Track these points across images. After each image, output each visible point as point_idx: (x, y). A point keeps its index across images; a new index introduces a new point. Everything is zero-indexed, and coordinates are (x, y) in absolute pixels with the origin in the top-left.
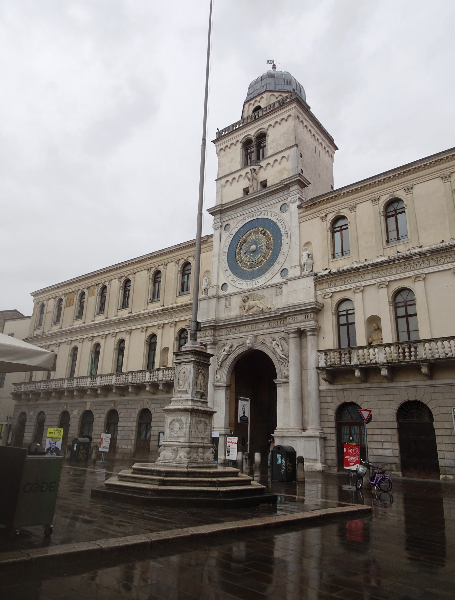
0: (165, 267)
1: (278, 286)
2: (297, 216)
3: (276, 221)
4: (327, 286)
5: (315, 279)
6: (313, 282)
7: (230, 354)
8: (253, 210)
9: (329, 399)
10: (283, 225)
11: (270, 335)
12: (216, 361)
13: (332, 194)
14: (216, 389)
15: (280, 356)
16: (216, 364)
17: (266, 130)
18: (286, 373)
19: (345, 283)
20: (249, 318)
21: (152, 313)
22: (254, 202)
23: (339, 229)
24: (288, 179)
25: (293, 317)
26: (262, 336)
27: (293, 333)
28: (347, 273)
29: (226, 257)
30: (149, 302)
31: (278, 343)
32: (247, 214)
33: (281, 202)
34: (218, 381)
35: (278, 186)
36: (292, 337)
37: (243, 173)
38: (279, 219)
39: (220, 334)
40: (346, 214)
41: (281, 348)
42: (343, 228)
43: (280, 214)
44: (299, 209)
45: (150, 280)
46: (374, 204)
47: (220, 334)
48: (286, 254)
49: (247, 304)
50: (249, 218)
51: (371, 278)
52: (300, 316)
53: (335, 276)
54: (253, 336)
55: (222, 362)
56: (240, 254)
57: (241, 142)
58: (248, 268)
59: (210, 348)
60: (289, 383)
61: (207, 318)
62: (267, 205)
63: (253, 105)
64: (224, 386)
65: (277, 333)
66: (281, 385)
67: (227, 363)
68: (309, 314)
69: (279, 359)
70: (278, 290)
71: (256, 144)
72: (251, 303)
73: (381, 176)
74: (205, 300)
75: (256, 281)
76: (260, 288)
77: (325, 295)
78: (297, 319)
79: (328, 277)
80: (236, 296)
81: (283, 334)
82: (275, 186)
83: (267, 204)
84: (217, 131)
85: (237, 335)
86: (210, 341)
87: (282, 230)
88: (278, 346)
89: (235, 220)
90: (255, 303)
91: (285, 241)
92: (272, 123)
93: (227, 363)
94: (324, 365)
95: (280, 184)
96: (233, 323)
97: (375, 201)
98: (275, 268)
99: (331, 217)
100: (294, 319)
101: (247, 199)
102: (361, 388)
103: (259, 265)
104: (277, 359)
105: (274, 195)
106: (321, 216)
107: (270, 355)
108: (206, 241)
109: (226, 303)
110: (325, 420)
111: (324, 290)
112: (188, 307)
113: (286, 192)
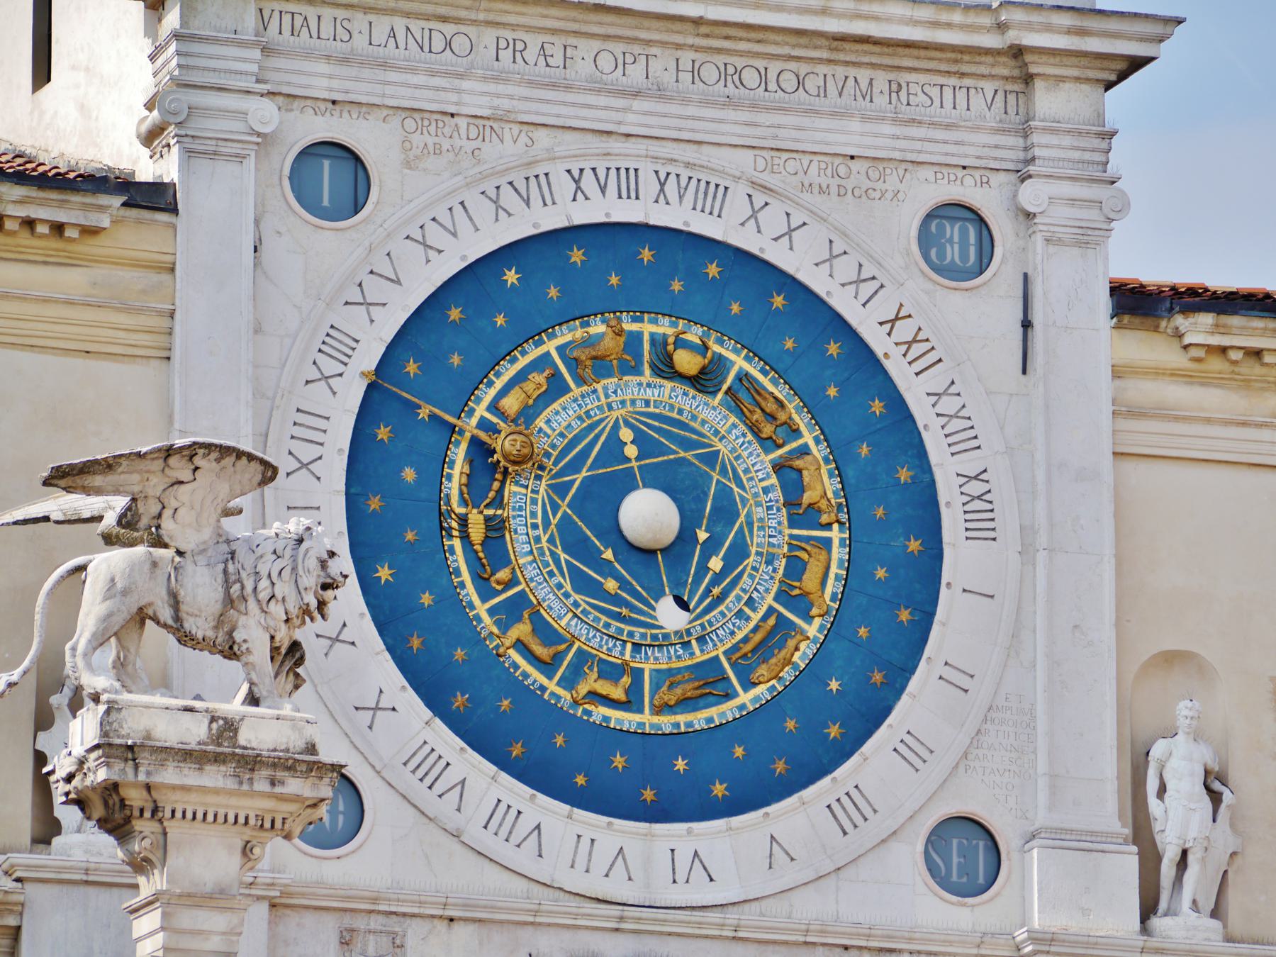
2: (1104, 386)
8: (631, 123)
10: (949, 405)
22: (648, 43)
24: (1065, 20)
33: (928, 173)
35: (949, 25)
38: (904, 331)
50: (588, 182)
80: (460, 930)
95: (972, 19)
105: (864, 75)
108: (90, 231)
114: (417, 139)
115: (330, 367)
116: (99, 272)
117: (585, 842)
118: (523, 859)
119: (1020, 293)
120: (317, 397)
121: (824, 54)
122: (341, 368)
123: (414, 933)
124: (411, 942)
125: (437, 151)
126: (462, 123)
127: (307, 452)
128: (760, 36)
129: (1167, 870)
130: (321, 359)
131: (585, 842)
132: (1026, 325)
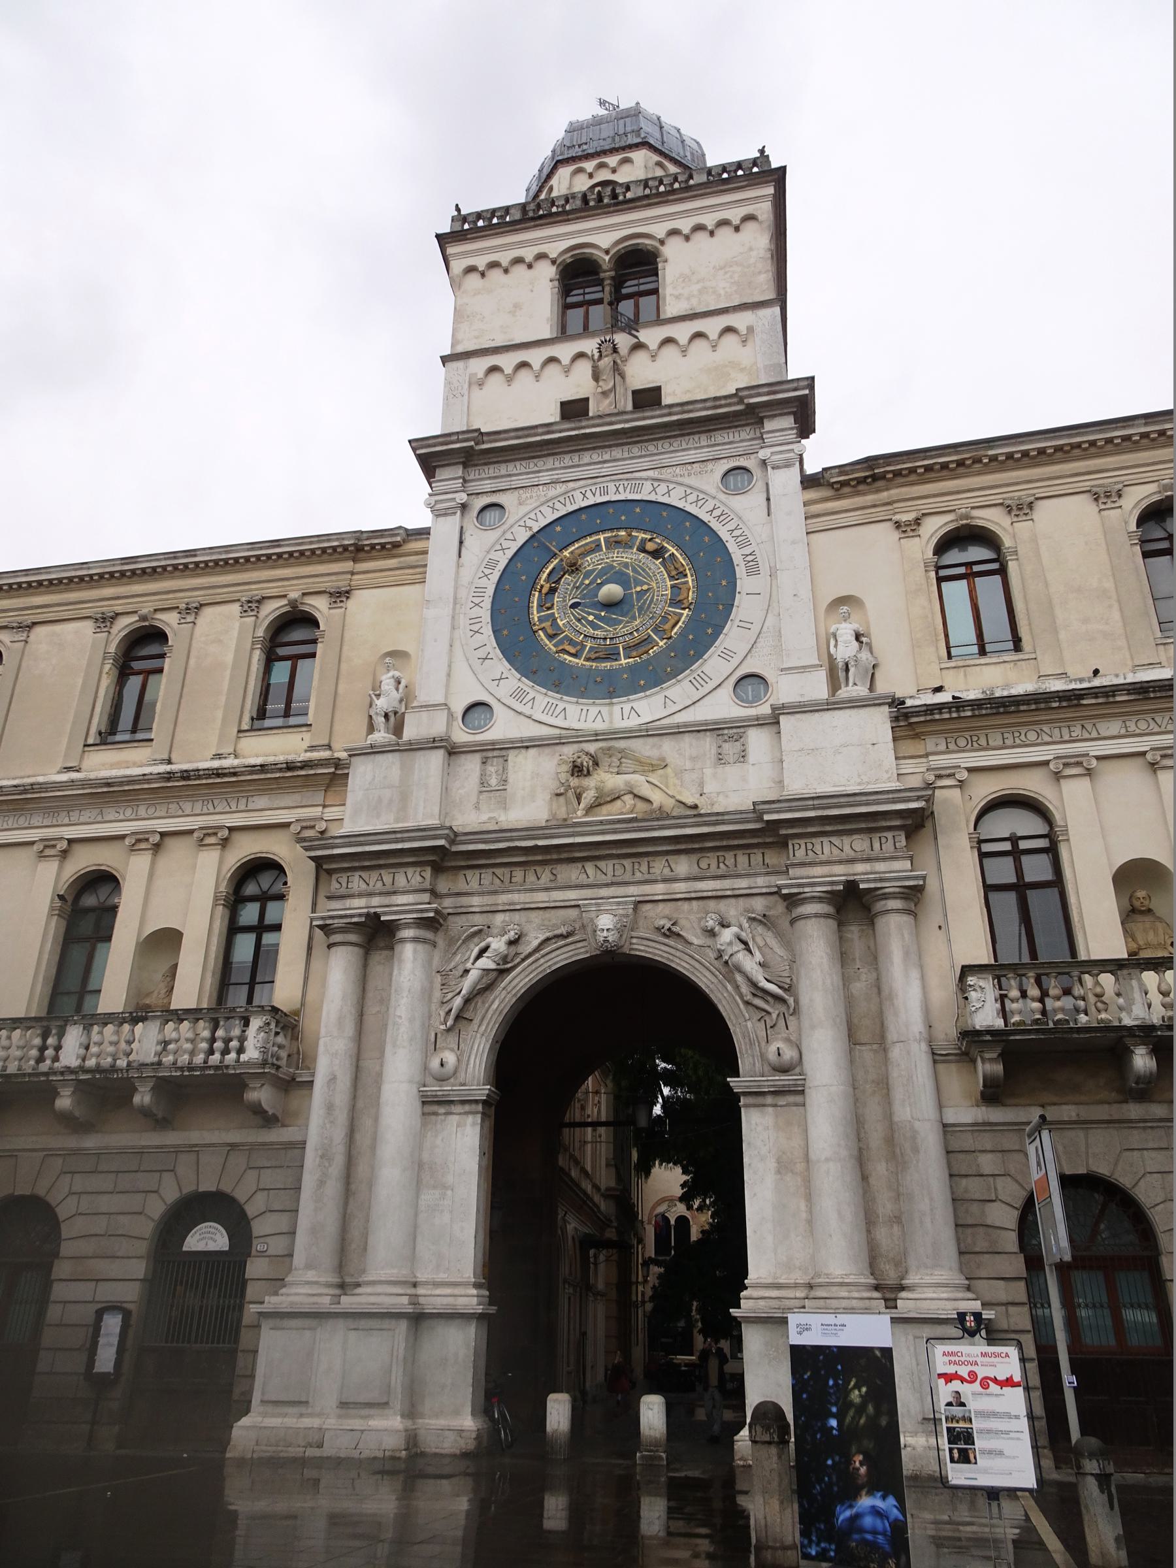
0: (190, 618)
1: (726, 731)
2: (800, 511)
3: (705, 517)
4: (942, 747)
5: (895, 719)
6: (888, 725)
7: (508, 971)
8: (604, 472)
9: (987, 1163)
10: (736, 533)
11: (701, 903)
12: (437, 994)
13: (949, 454)
14: (435, 1114)
15: (754, 984)
16: (433, 1007)
17: (657, 244)
18: (789, 1054)
19: (1018, 741)
20: (615, 832)
21: (108, 785)
22: (610, 446)
23: (962, 570)
24: (765, 390)
25: (815, 841)
26: (661, 906)
27: (819, 900)
28: (1033, 707)
29: (485, 614)
30: (90, 741)
31: (743, 935)
32: (582, 483)
33: (725, 461)
34: (442, 1080)
36: (817, 916)
37: (565, 351)
38: (717, 513)
39: (461, 886)
40: (997, 524)
41: (758, 956)
42: (976, 568)
43: (722, 497)
44: (804, 488)
45: (104, 658)
46: (1103, 507)
47: (461, 886)
48: (755, 629)
49: (591, 782)
50: (589, 494)
51: (1123, 731)
52: (847, 840)
53: (984, 712)
54: (626, 903)
55: (467, 1001)
56: (548, 609)
57: (554, 262)
58: (587, 659)
59: (416, 940)
60: (802, 1092)
61: (397, 821)
62: (666, 462)
63: (591, 176)
64: (476, 1102)
65: (733, 901)
66: (760, 1100)
67: (495, 1006)
68: (889, 835)
69: (749, 997)
70: (726, 746)
71: (612, 278)
72: (607, 779)
73: (1136, 422)
74: (390, 755)
75: (627, 707)
76: (648, 732)
77: (939, 777)
78: (836, 851)
79: (954, 715)
80: (532, 751)
81: (759, 904)
82: (709, 404)
83: (666, 459)
84: (456, 213)
85: (541, 897)
86: (422, 911)
87: (732, 547)
88: (743, 946)
89: (524, 494)
90: (627, 783)
91: (745, 583)
92: (685, 225)
93: (495, 1006)
94: (999, 1023)
95: (729, 401)
96: (537, 847)
97: (1104, 497)
98: (707, 668)
99: (935, 527)
100: (818, 848)
101: (588, 431)
102: (1131, 1121)
103: (634, 654)
104: (741, 996)
105: (696, 437)
106: (897, 517)
107: (706, 980)
108: (396, 545)
109: (483, 774)
110: (977, 1249)
111: (931, 758)
112: (303, 773)
113: (746, 433)
114: (524, 496)
115: (487, 571)
116: (402, 559)
117: (584, 712)
118: (559, 722)
119: (765, 489)
120: (484, 582)
121: (678, 433)
122: (491, 571)
123: (512, 755)
124: (510, 758)
125: (531, 497)
126: (541, 487)
127: (477, 600)
128: (650, 432)
129: (842, 675)
130: (485, 570)
131: (584, 712)
132: (768, 499)
